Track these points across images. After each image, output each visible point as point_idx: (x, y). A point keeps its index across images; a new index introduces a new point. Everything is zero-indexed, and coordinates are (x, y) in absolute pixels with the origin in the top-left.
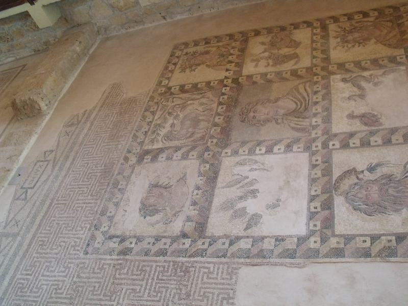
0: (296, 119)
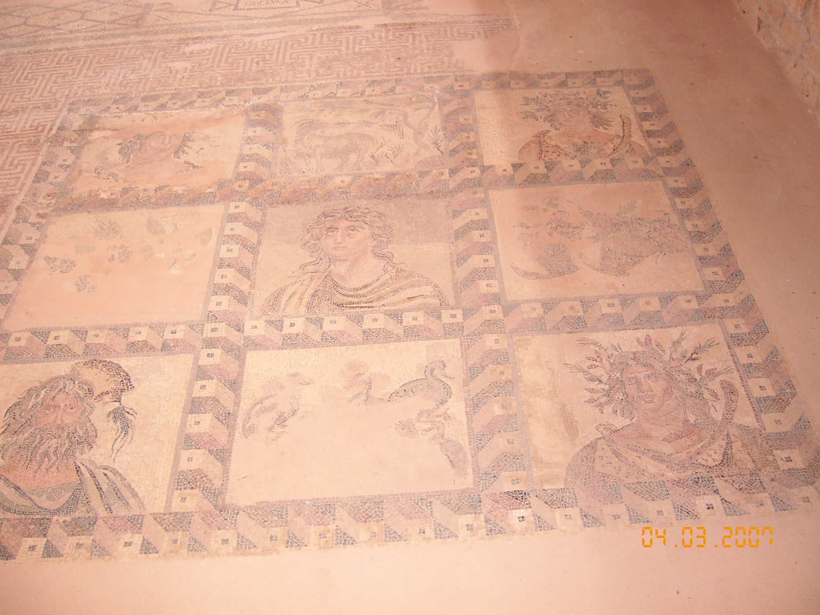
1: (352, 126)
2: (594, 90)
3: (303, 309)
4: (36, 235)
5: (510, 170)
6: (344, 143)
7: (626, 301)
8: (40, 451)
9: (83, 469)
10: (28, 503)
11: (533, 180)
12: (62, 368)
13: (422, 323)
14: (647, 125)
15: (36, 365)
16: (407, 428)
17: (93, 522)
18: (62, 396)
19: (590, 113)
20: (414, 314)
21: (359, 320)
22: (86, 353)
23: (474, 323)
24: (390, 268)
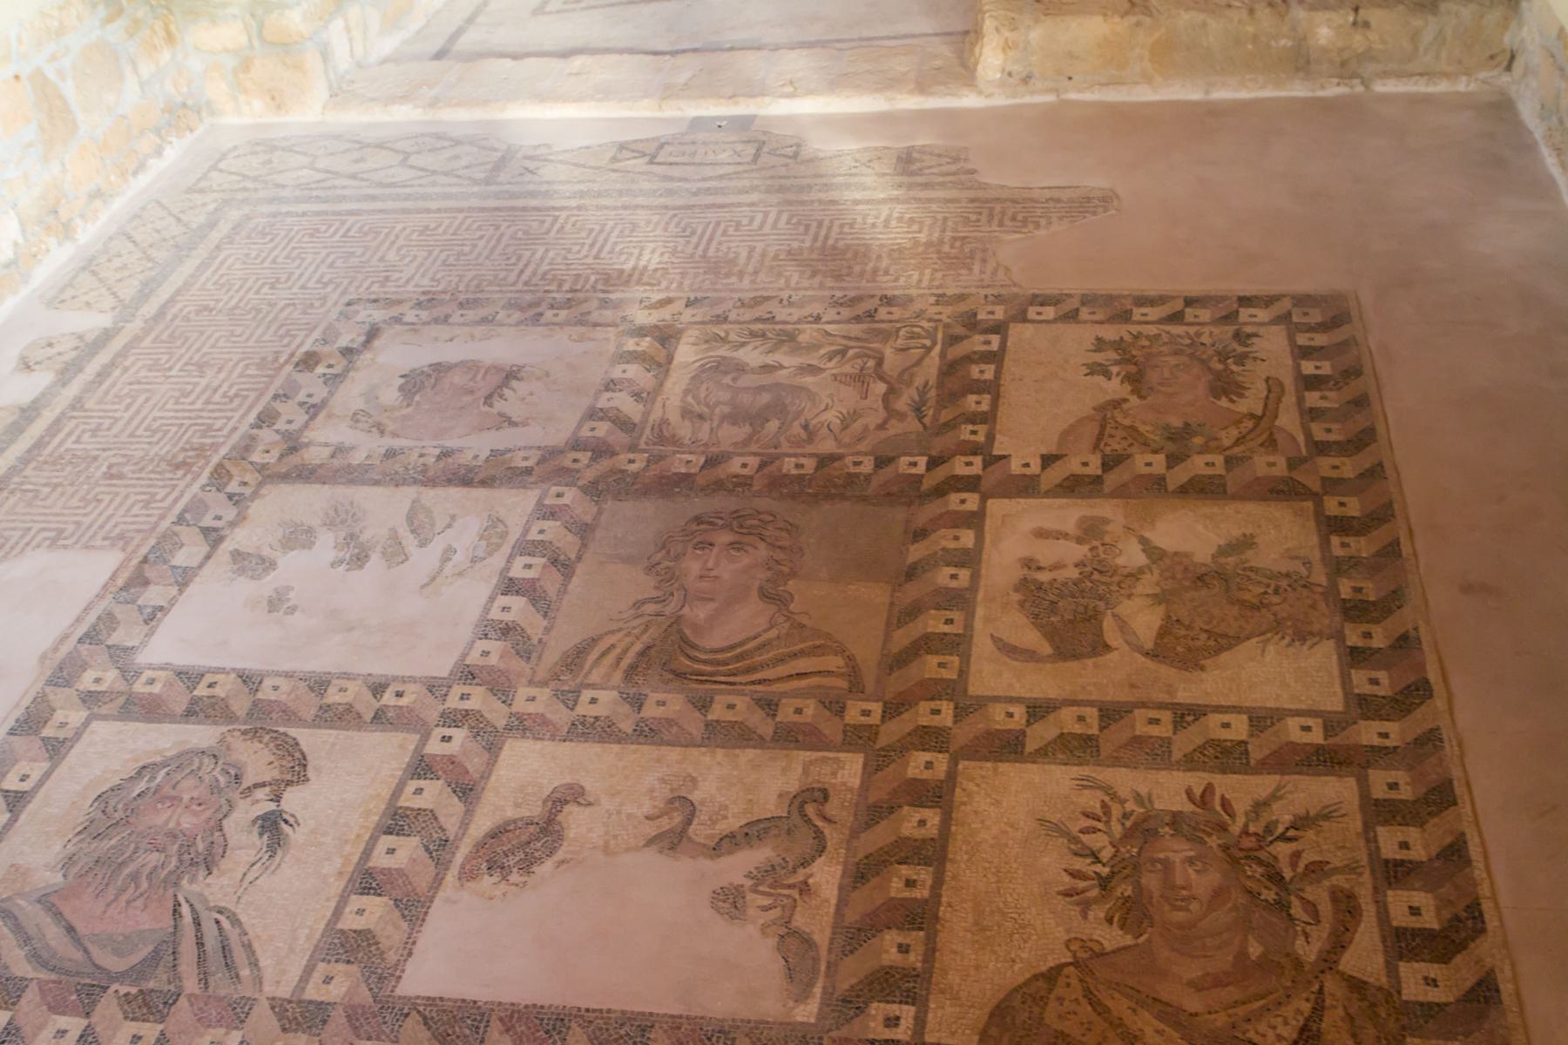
0: (638, 647)
1: (784, 372)
2: (1230, 330)
3: (618, 676)
4: (230, 513)
5: (1035, 468)
6: (765, 398)
7: (1186, 715)
8: (127, 871)
9: (185, 910)
10: (79, 955)
11: (1073, 487)
12: (202, 735)
13: (809, 720)
14: (1313, 398)
15: (167, 727)
16: (730, 901)
17: (171, 1000)
18: (191, 782)
19: (1210, 369)
20: (798, 702)
21: (703, 705)
22: (250, 714)
23: (893, 731)
24: (781, 619)
